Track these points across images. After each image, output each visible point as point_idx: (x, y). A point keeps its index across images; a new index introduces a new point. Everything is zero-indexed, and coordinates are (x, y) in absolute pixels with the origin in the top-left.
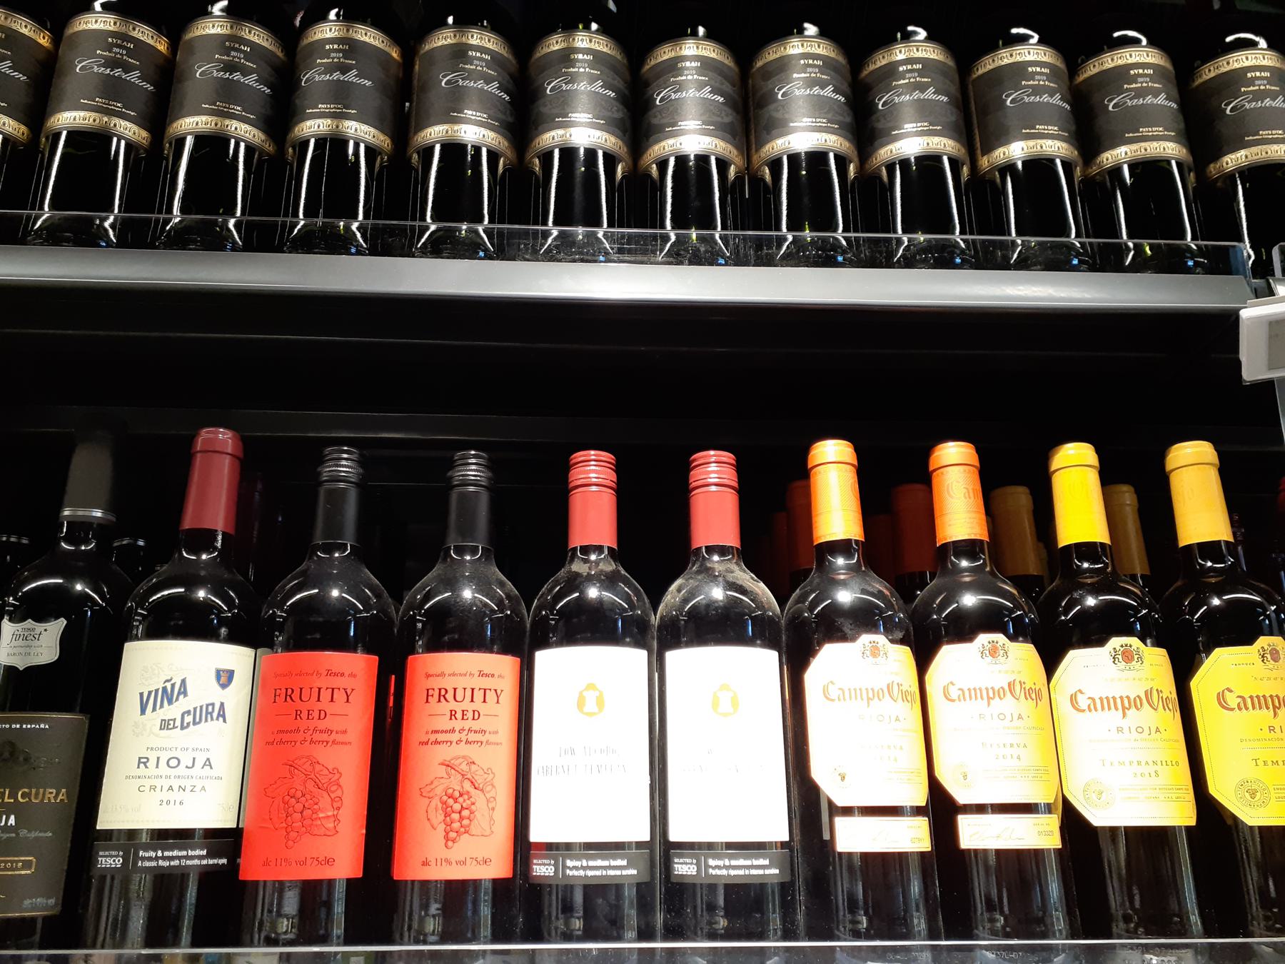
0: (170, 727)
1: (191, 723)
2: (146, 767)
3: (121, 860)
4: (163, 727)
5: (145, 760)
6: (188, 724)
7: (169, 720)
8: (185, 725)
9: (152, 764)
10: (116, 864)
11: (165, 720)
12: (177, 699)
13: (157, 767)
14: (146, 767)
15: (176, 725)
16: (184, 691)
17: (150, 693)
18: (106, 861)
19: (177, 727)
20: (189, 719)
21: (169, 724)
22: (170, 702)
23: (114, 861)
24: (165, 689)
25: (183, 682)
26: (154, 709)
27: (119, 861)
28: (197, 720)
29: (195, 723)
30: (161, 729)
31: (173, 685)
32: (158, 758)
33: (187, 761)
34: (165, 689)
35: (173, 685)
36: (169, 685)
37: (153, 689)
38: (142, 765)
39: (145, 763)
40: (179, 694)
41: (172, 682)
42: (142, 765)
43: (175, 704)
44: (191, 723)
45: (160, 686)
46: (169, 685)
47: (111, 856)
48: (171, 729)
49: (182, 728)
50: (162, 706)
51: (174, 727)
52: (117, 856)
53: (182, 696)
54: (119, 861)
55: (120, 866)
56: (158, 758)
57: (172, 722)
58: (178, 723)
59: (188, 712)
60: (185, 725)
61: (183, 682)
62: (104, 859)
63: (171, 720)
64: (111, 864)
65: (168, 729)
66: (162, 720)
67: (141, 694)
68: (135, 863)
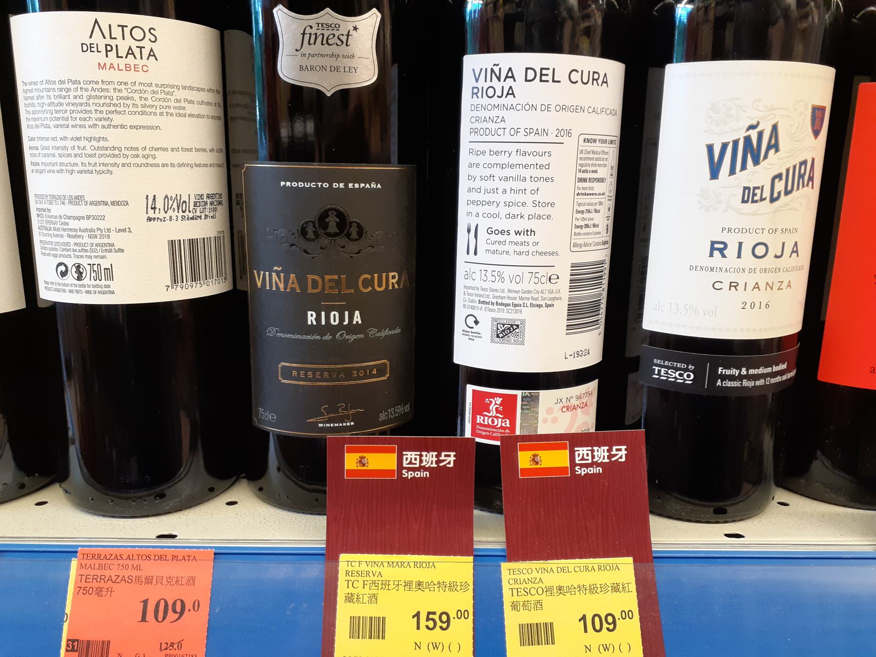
0: (756, 198)
1: (783, 193)
2: (724, 256)
3: (692, 376)
4: (746, 199)
5: (722, 246)
6: (779, 193)
7: (755, 188)
8: (775, 195)
9: (731, 251)
10: (684, 379)
11: (749, 188)
12: (766, 157)
13: (739, 256)
14: (724, 256)
15: (764, 197)
16: (774, 146)
17: (724, 146)
18: (667, 373)
19: (765, 199)
20: (780, 186)
21: (754, 195)
22: (756, 162)
23: (681, 375)
24: (748, 139)
25: (775, 128)
26: (732, 172)
27: (688, 376)
28: (789, 188)
29: (787, 193)
30: (743, 201)
31: (760, 135)
32: (740, 244)
33: (775, 249)
34: (748, 139)
35: (760, 135)
36: (754, 134)
37: (730, 138)
38: (716, 253)
39: (721, 251)
40: (769, 147)
41: (759, 129)
42: (716, 253)
43: (763, 164)
44: (783, 193)
45: (741, 135)
46: (754, 134)
47: (677, 369)
48: (756, 202)
49: (773, 200)
50: (744, 167)
51: (762, 199)
52: (686, 370)
53: (772, 151)
54: (688, 376)
55: (690, 382)
56: (740, 244)
57: (758, 192)
58: (767, 194)
59: (779, 176)
60: (775, 195)
61: (775, 128)
62: (663, 369)
63: (758, 188)
64: (675, 378)
65: (754, 201)
66: (745, 188)
67: (710, 148)
68: (713, 381)
